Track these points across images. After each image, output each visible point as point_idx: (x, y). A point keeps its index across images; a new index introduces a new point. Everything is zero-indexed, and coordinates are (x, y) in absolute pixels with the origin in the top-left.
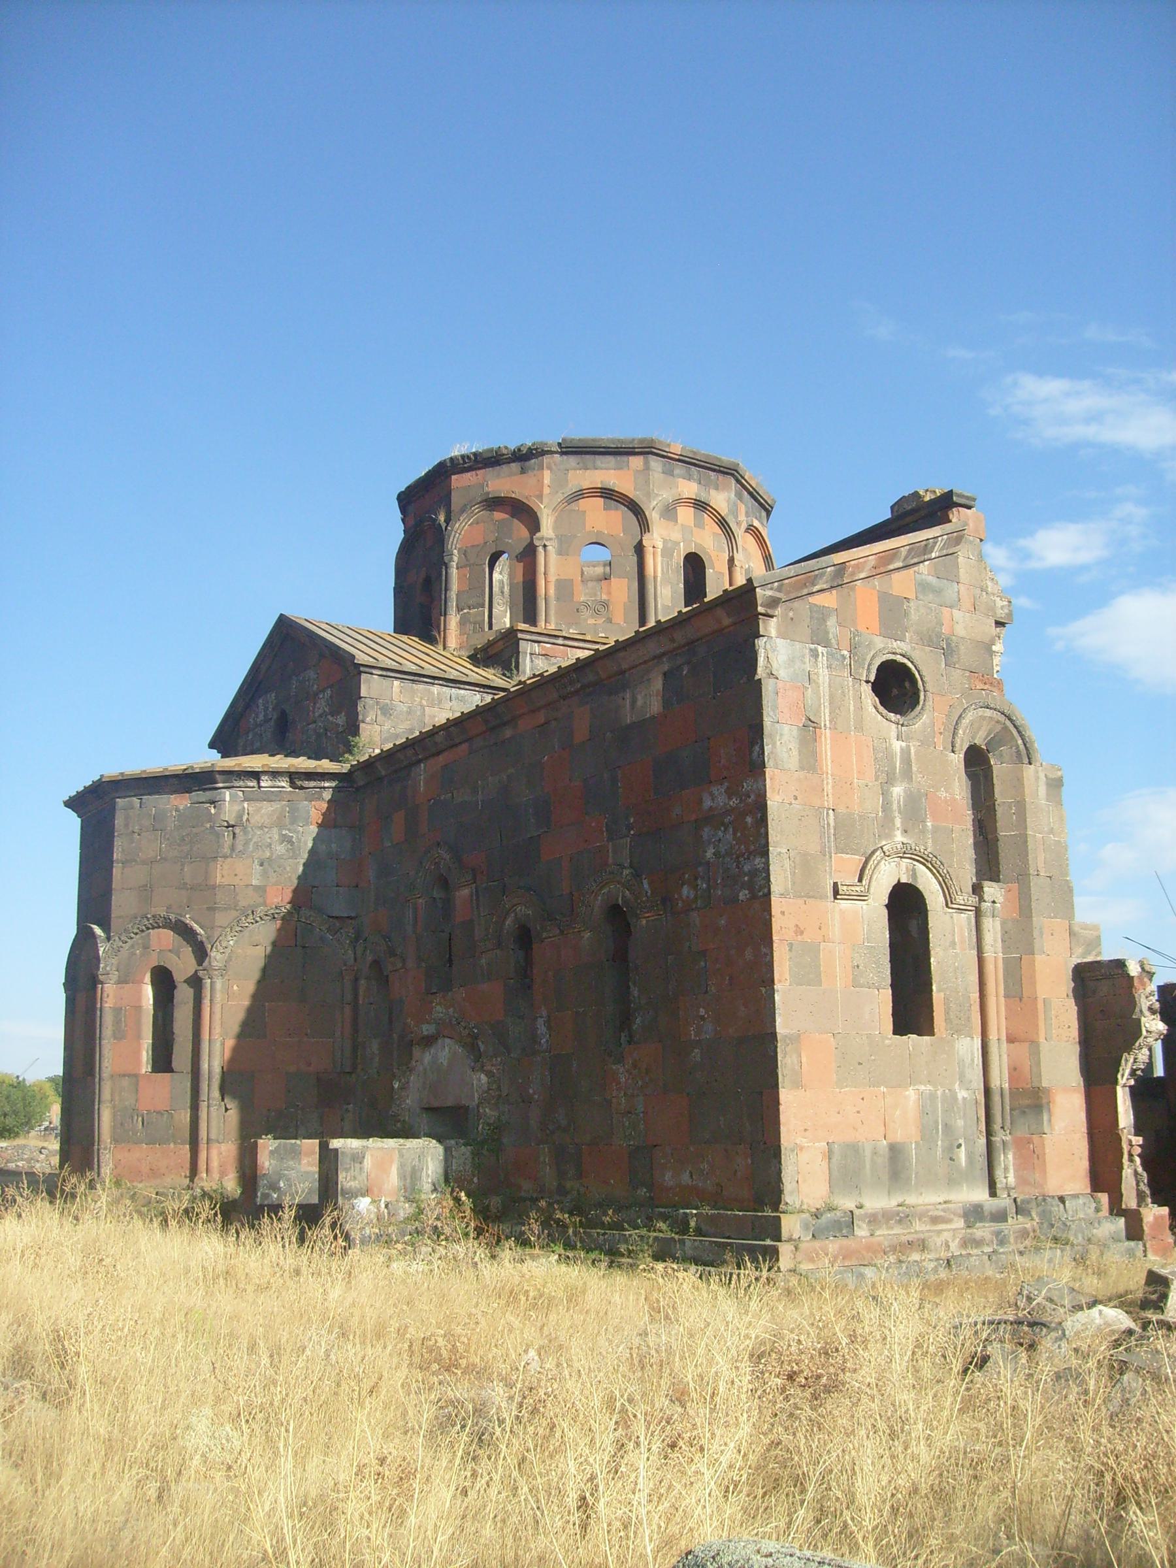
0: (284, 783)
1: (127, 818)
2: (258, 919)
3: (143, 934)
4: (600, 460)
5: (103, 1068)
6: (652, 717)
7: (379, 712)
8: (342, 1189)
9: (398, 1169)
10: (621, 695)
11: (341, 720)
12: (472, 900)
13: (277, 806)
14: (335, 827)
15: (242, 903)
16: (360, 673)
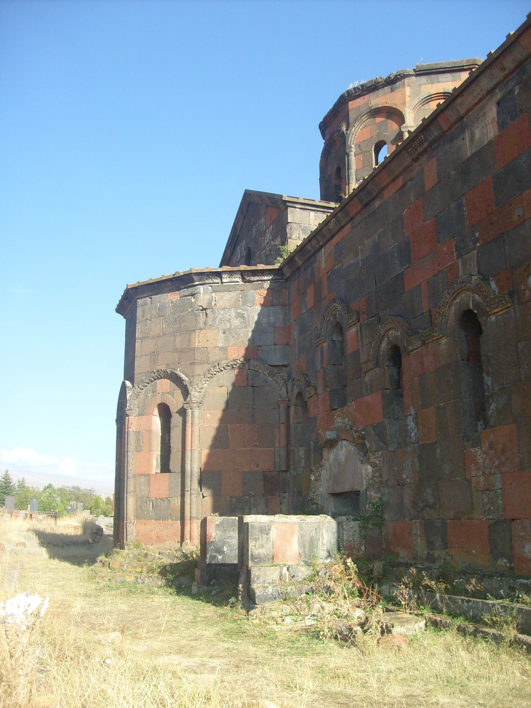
0: (238, 279)
1: (143, 311)
2: (222, 369)
3: (153, 383)
4: (441, 77)
5: (129, 471)
6: (490, 143)
7: (301, 232)
8: (252, 555)
9: (298, 539)
10: (461, 137)
11: (278, 241)
12: (357, 335)
13: (233, 294)
14: (272, 305)
15: (212, 359)
16: (287, 207)
